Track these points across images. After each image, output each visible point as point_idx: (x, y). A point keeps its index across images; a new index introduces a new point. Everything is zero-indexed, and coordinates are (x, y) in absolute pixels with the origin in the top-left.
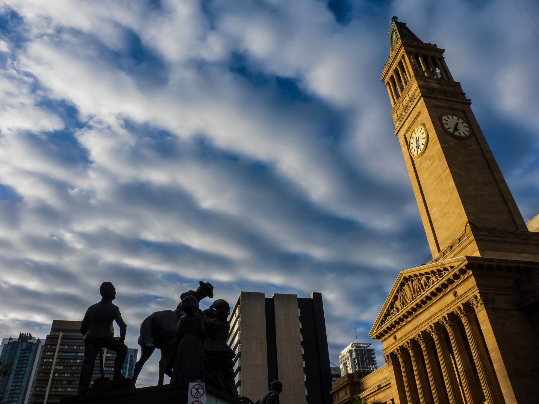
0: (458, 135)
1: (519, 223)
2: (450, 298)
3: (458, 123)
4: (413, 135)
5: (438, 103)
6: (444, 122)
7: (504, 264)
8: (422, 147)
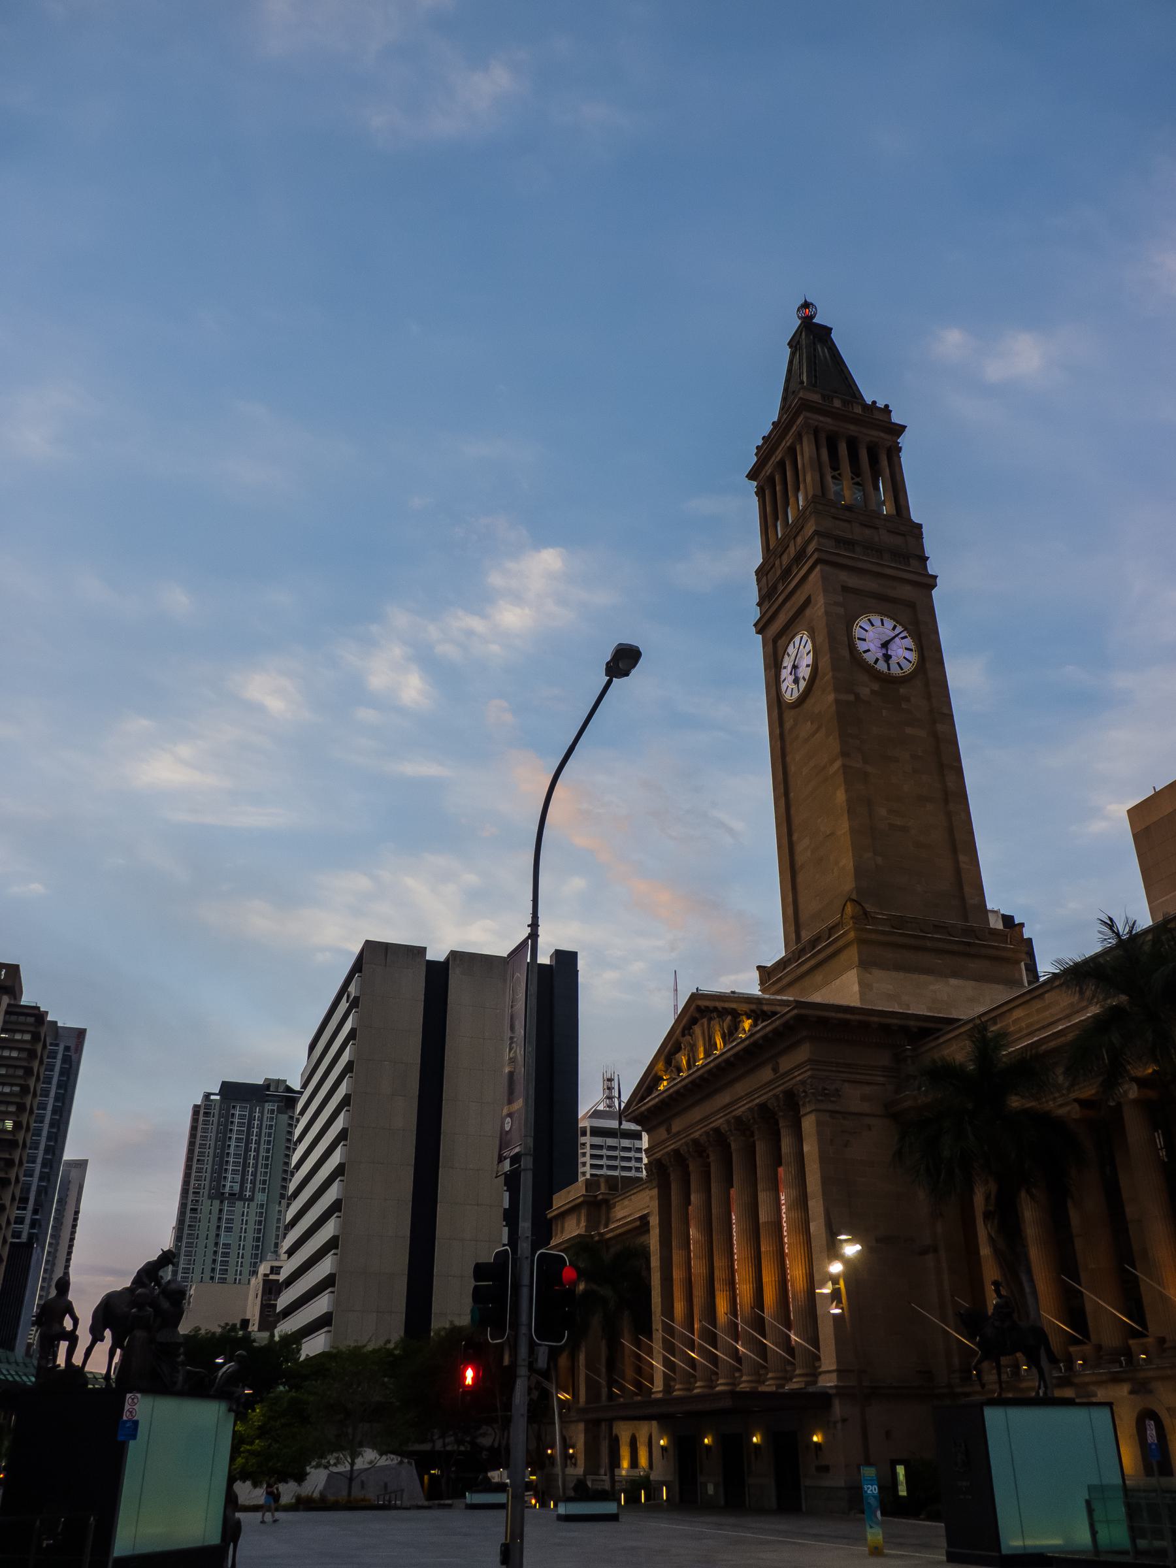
0: (886, 670)
2: (766, 1074)
5: (853, 581)
8: (803, 684)
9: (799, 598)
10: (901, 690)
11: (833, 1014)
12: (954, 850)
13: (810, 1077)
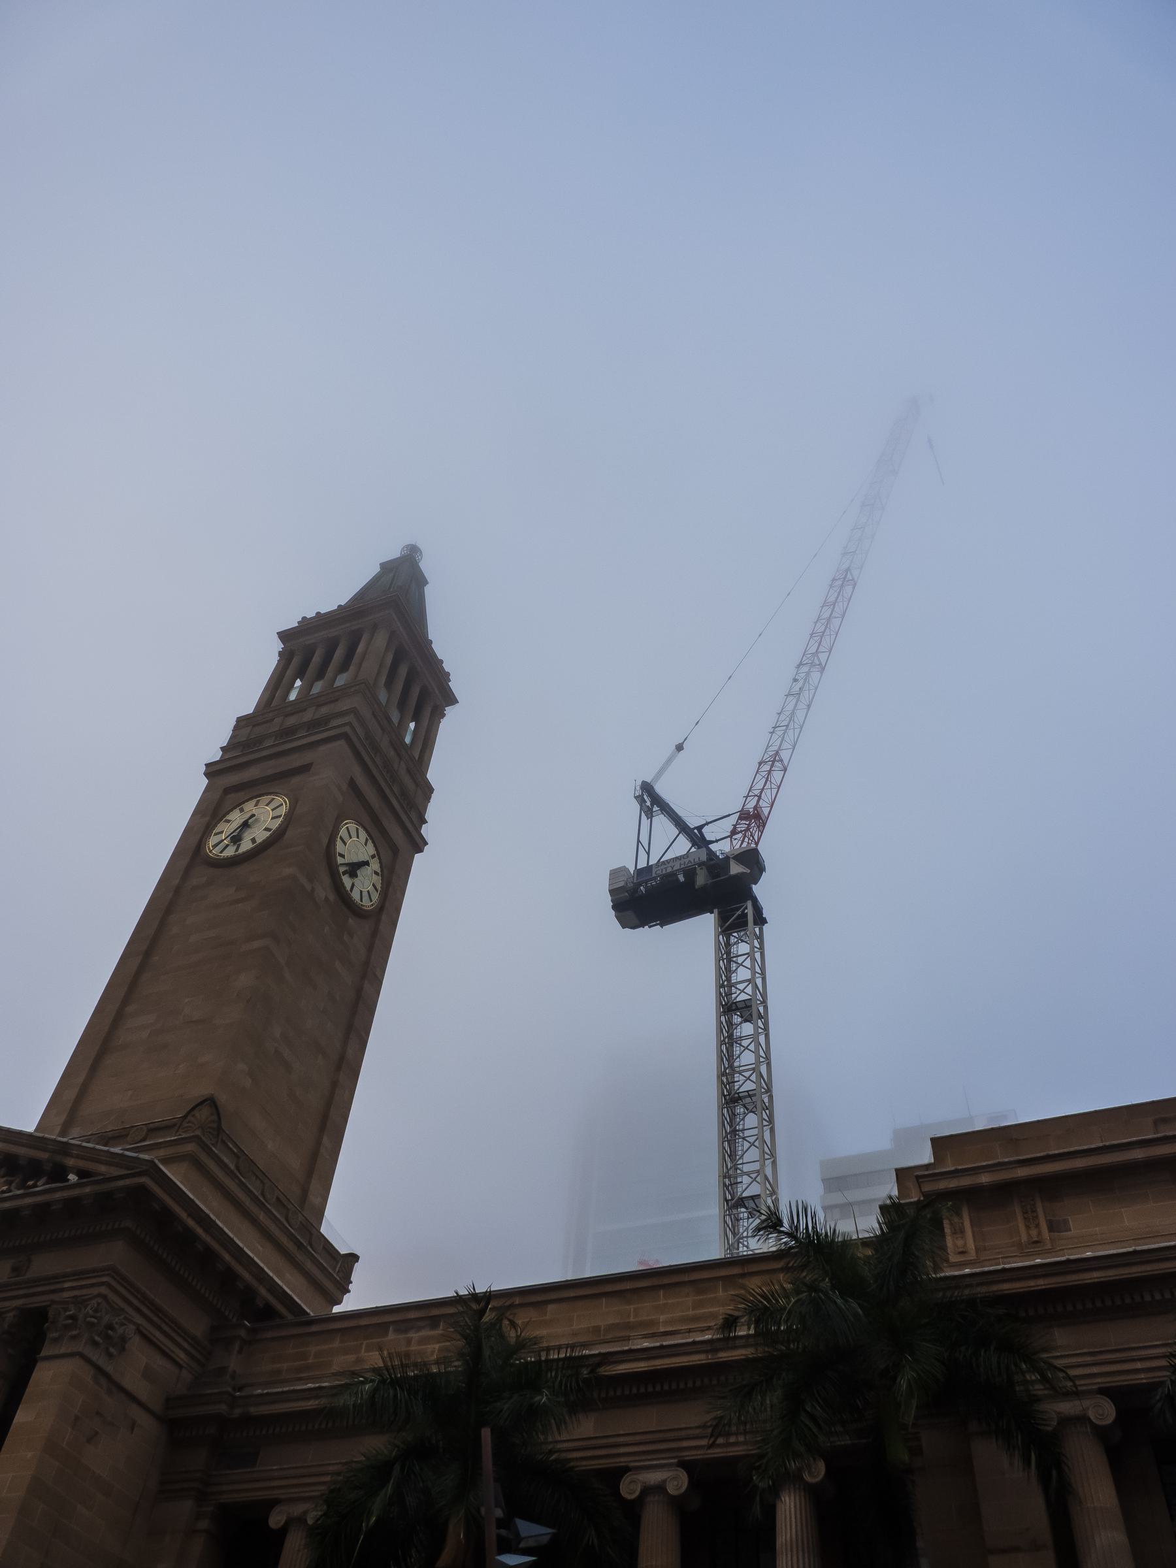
0: (348, 888)
1: (314, 1199)
3: (367, 863)
4: (249, 807)
6: (343, 832)
7: (227, 1257)
8: (246, 845)
9: (296, 761)
10: (350, 920)
11: (183, 1215)
12: (322, 1129)
13: (99, 1295)
